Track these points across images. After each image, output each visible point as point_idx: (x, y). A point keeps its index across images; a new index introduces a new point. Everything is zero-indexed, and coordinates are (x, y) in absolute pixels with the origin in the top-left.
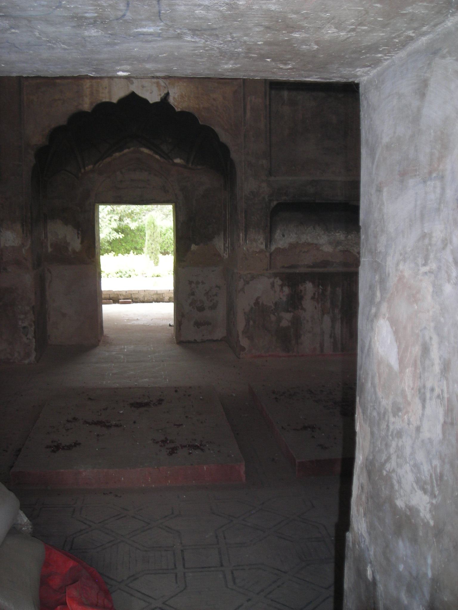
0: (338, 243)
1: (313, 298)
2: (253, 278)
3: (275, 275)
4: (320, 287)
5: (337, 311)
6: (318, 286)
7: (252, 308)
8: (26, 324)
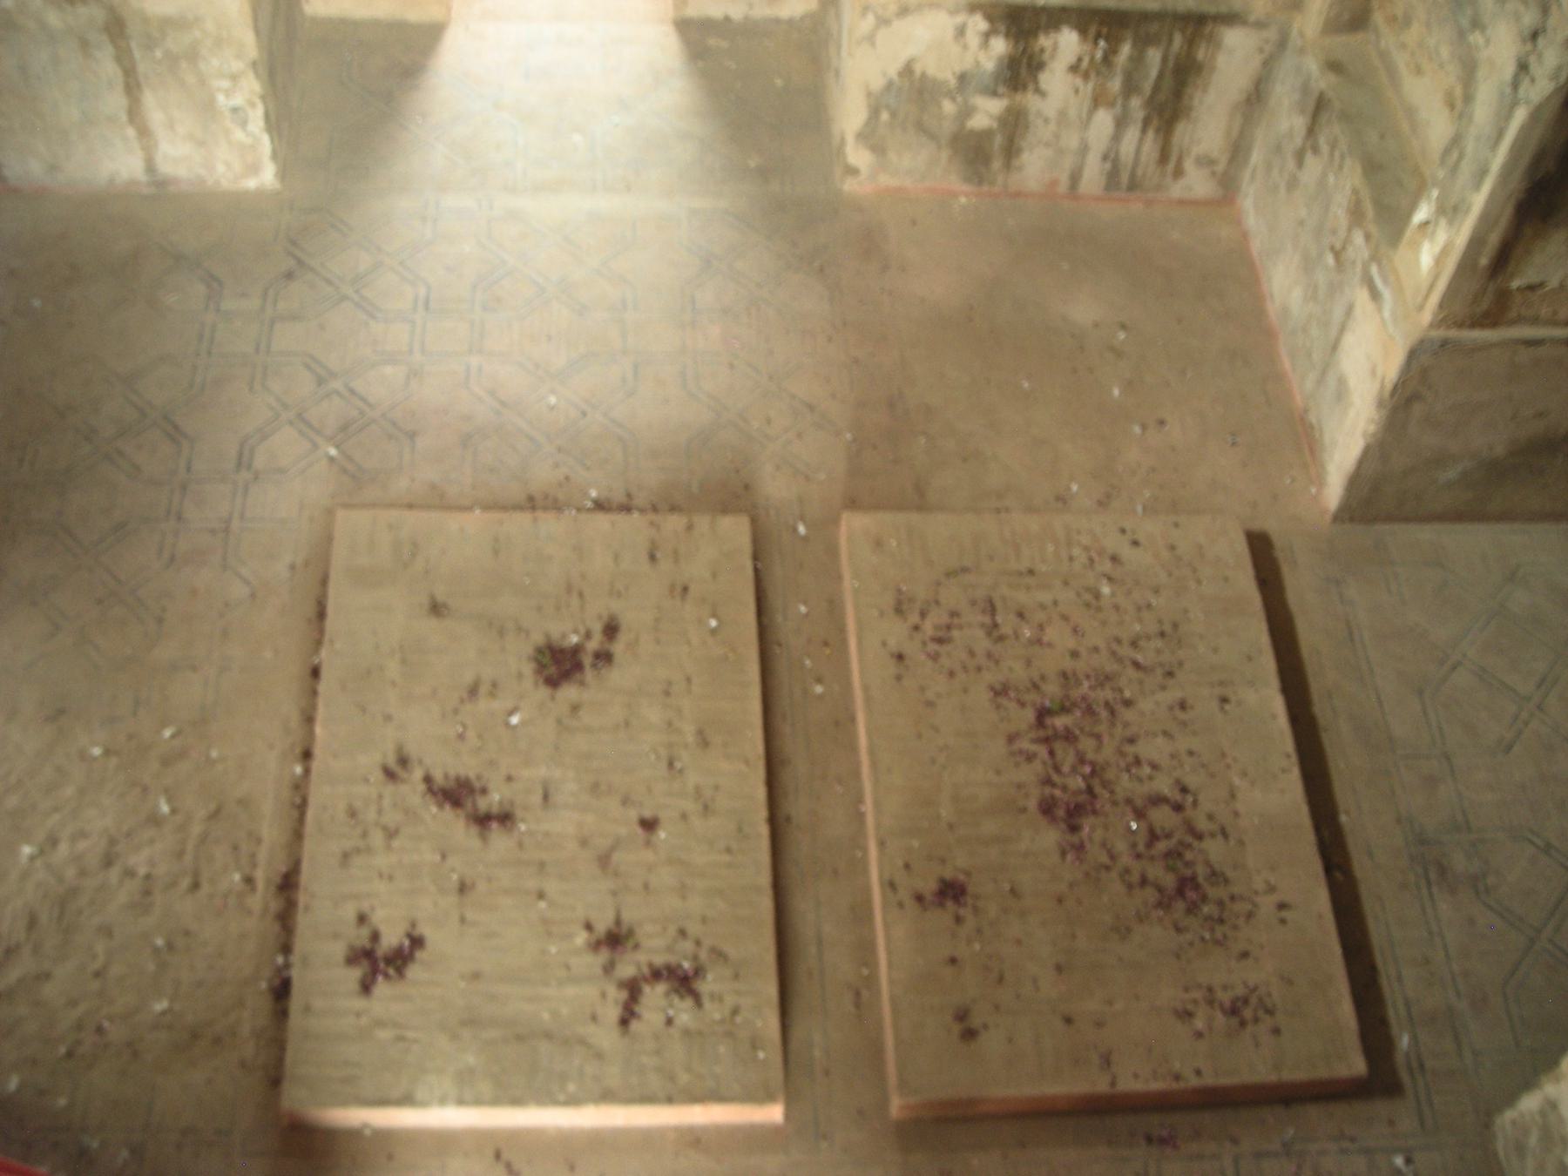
1: (1074, 69)
4: (1102, 43)
5: (1136, 102)
6: (1096, 43)
7: (889, 86)
8: (238, 100)
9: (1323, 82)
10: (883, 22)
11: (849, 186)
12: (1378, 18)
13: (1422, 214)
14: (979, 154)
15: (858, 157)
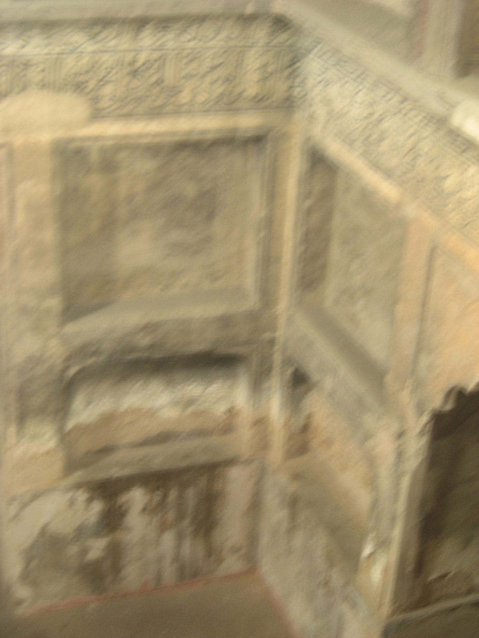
0: (190, 402)
1: (144, 510)
2: (36, 496)
3: (78, 486)
9: (293, 487)
10: (24, 506)
11: (20, 611)
12: (315, 443)
13: (367, 550)
14: (98, 575)
15: (22, 592)
